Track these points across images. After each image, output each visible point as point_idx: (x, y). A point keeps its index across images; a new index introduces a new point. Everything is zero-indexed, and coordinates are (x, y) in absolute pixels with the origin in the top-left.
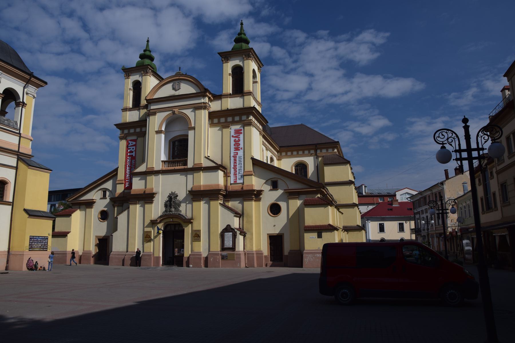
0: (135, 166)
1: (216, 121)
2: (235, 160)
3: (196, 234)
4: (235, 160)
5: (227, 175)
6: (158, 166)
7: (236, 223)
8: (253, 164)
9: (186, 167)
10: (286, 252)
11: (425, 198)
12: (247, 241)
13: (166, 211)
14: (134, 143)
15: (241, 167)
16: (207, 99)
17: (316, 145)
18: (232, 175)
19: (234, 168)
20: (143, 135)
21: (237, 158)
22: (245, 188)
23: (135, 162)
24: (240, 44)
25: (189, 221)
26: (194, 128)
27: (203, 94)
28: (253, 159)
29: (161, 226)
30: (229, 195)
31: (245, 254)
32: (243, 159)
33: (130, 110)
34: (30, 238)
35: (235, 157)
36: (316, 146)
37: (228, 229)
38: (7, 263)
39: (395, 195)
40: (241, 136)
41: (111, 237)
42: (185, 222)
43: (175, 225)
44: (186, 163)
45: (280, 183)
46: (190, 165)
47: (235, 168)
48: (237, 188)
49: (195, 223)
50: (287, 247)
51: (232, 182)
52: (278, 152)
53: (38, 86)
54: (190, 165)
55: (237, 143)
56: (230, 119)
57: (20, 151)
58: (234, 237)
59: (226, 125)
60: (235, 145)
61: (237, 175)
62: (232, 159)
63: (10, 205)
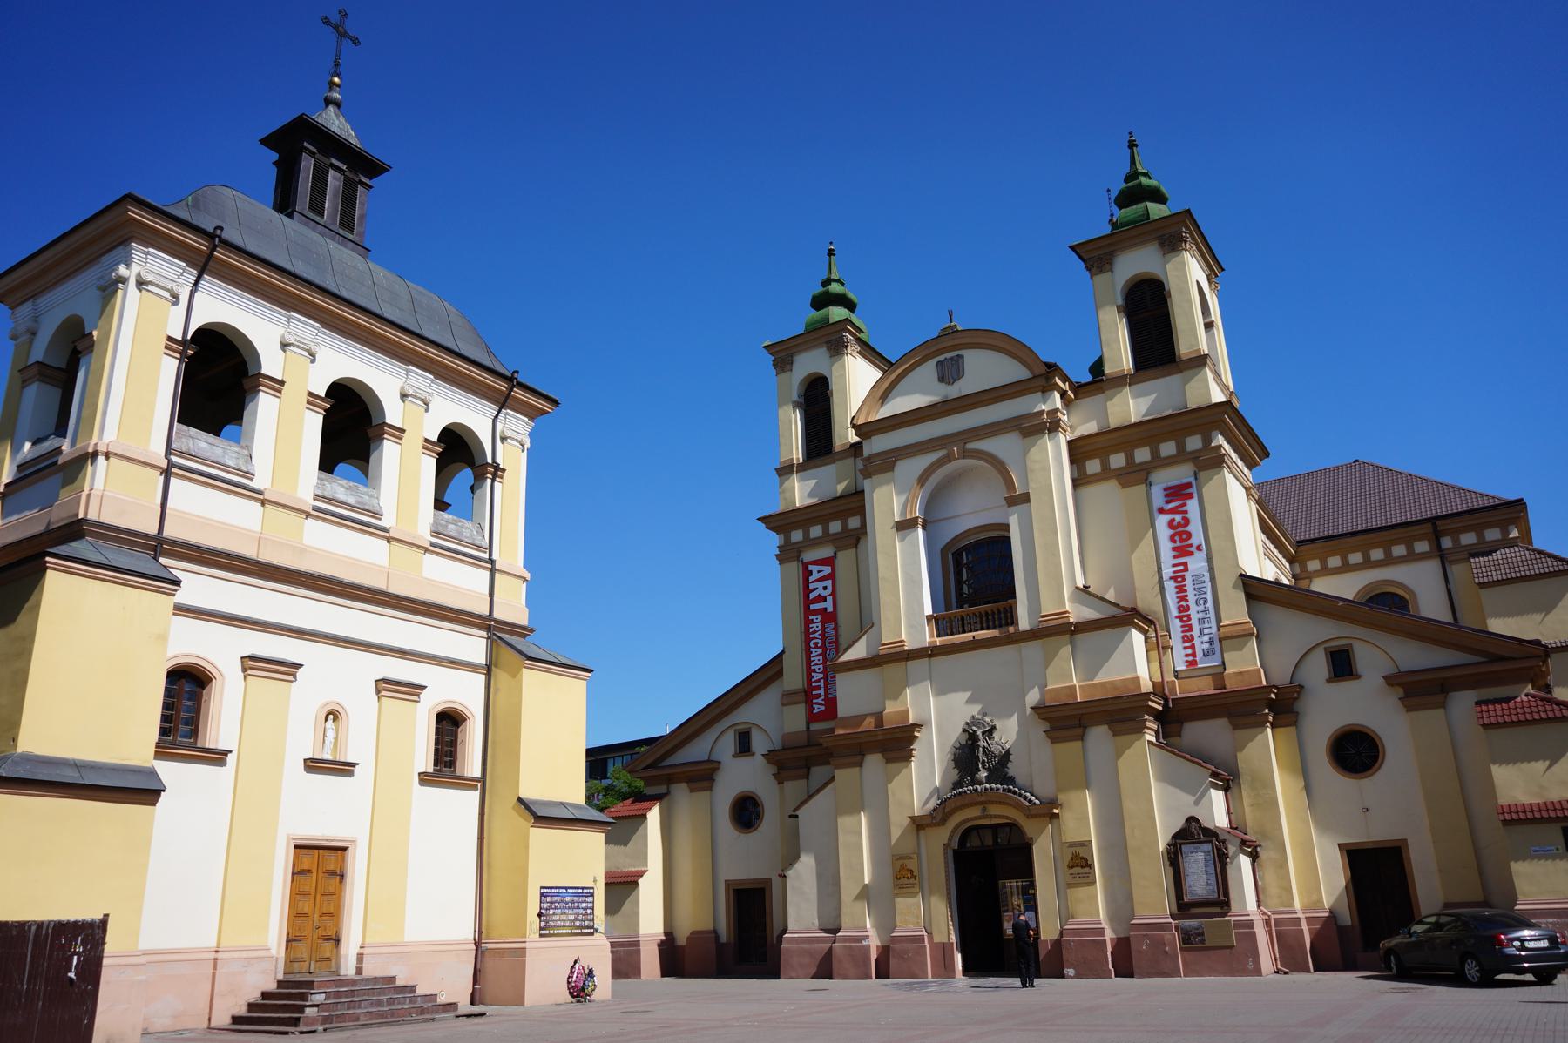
0: (836, 642)
1: (1093, 466)
2: (1181, 589)
3: (1075, 857)
4: (1181, 589)
5: (1158, 648)
7: (1216, 809)
8: (1250, 597)
9: (1011, 629)
12: (1269, 876)
13: (958, 784)
14: (827, 570)
15: (1206, 611)
16: (1057, 396)
18: (1176, 642)
19: (1179, 617)
20: (856, 538)
21: (1189, 582)
22: (1231, 686)
23: (836, 629)
24: (1138, 208)
25: (1048, 811)
27: (1042, 382)
28: (1243, 576)
30: (1174, 716)
31: (1267, 923)
32: (1208, 585)
33: (802, 468)
34: (542, 895)
35: (1178, 579)
36: (1435, 526)
37: (1191, 833)
38: (475, 981)
40: (1192, 506)
41: (776, 882)
42: (1030, 816)
43: (995, 828)
44: (1010, 617)
47: (1184, 616)
48: (1204, 687)
49: (1068, 819)
50: (1430, 889)
51: (1181, 666)
52: (1291, 562)
53: (532, 413)
56: (1142, 455)
57: (496, 615)
58: (1221, 860)
60: (1172, 539)
61: (1197, 641)
62: (1170, 586)
63: (474, 788)
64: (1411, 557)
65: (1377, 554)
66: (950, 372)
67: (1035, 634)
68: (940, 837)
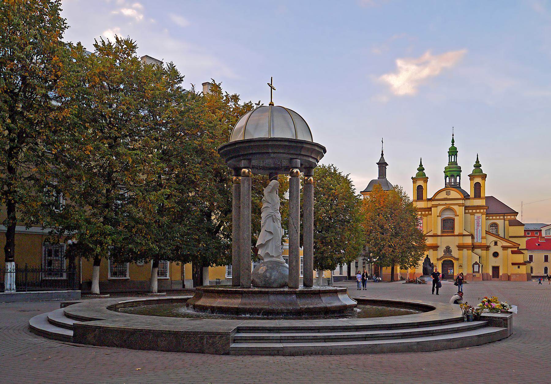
1: (467, 211)
6: (439, 234)
10: (501, 274)
17: (504, 214)
26: (458, 216)
37: (476, 263)
44: (453, 232)
45: (499, 243)
46: (456, 233)
47: (477, 235)
54: (456, 233)
55: (478, 223)
56: (474, 211)
58: (479, 267)
59: (472, 214)
64: (500, 219)
65: (494, 218)
66: (448, 194)
68: (442, 261)
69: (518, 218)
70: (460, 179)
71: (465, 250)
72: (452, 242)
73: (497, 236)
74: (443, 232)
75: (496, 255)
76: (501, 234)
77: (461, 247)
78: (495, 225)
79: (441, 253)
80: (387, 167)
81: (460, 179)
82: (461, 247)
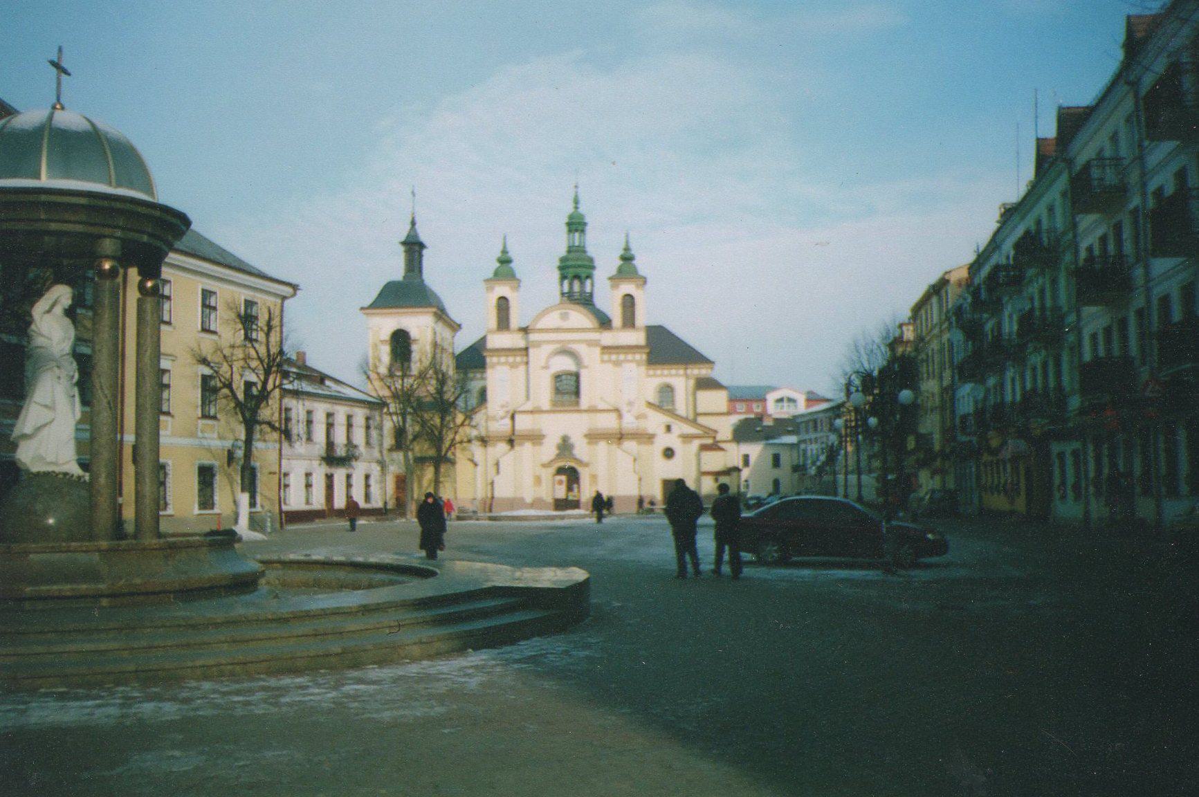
1: (606, 357)
11: (815, 422)
29: (552, 470)
39: (765, 400)
44: (577, 403)
45: (674, 428)
56: (622, 357)
59: (617, 363)
65: (666, 372)
66: (564, 317)
67: (586, 411)
69: (717, 373)
70: (592, 285)
71: (602, 445)
72: (572, 425)
73: (672, 413)
74: (555, 403)
75: (669, 453)
76: (681, 406)
77: (593, 437)
78: (667, 391)
79: (549, 450)
80: (425, 252)
81: (592, 285)
82: (593, 437)
